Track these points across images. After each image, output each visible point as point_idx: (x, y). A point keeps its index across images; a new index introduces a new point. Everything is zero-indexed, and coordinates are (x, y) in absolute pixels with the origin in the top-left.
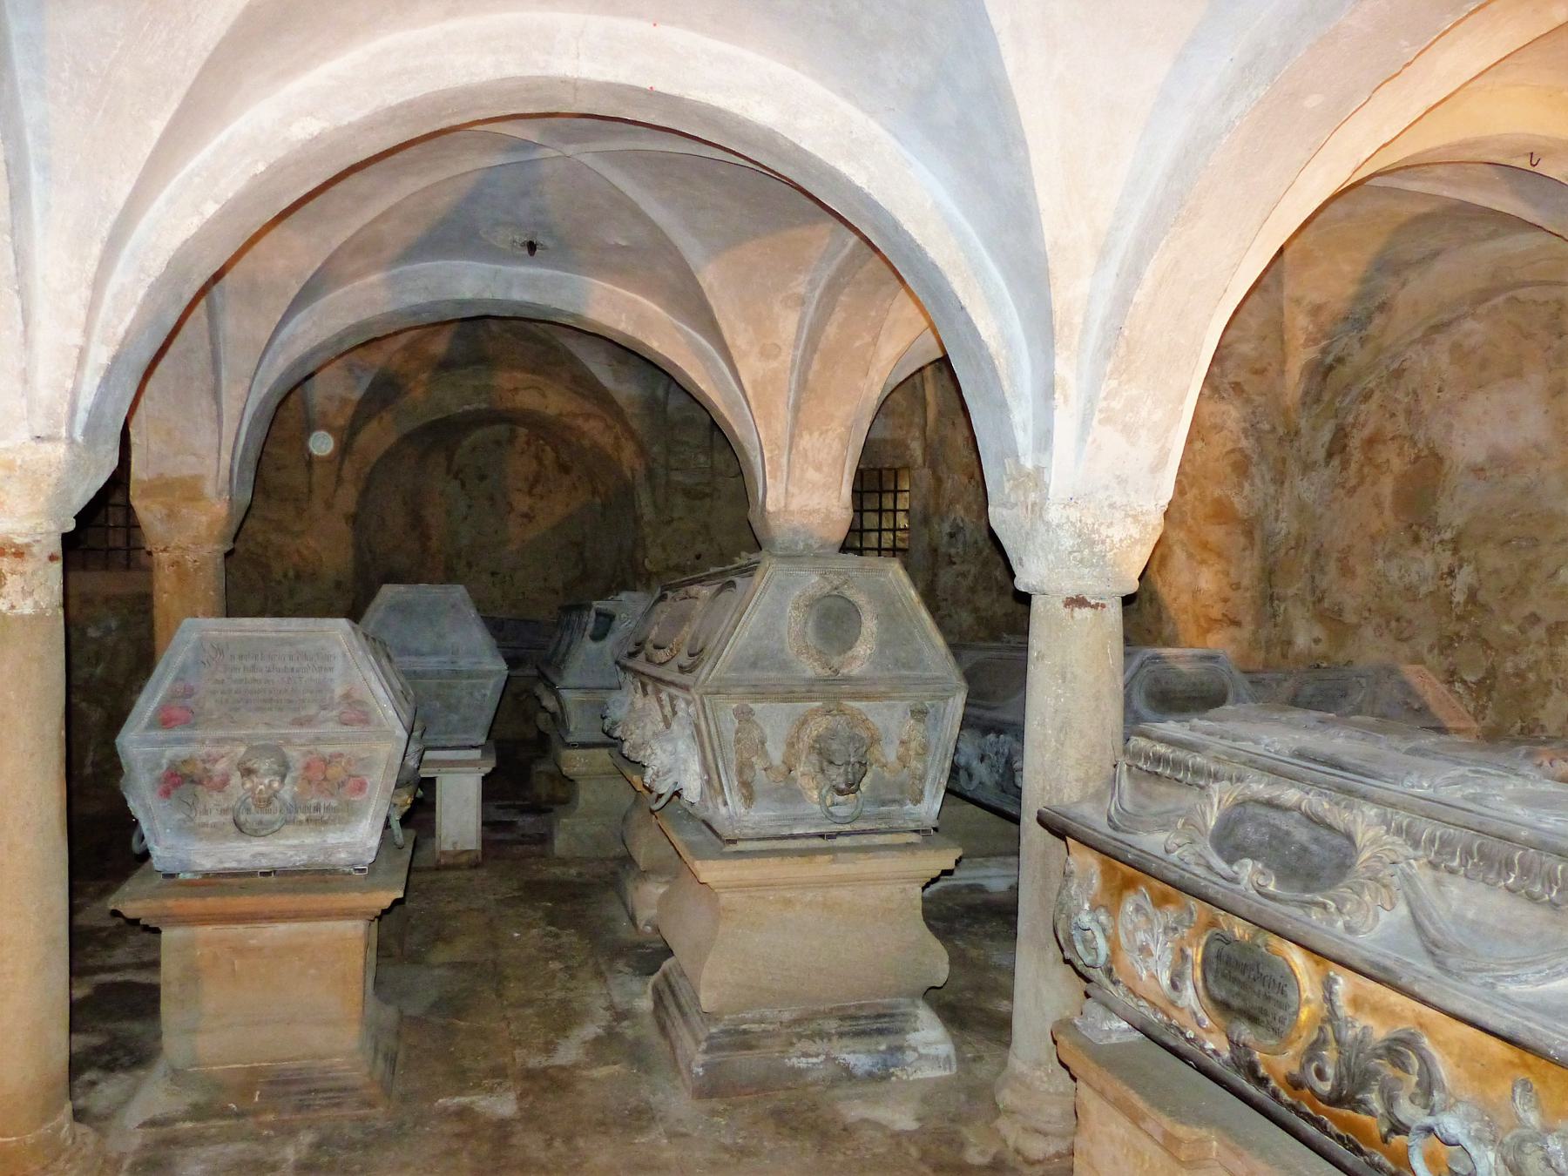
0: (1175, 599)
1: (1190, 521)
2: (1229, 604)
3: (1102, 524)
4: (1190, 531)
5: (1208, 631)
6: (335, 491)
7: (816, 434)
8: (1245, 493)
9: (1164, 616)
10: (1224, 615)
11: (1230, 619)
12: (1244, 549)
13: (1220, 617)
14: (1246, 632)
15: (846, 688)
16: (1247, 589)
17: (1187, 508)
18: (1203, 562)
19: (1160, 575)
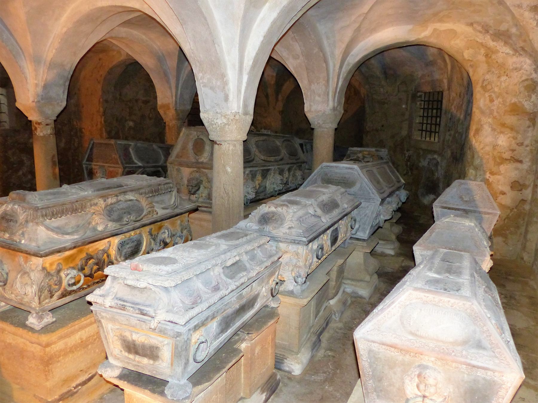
0: (482, 149)
1: (495, 114)
2: (516, 152)
3: (214, 119)
4: (495, 118)
5: (501, 163)
6: (276, 104)
7: (316, 84)
8: (532, 100)
9: (476, 157)
10: (511, 157)
11: (515, 159)
12: (529, 127)
13: (509, 158)
14: (525, 166)
15: (201, 165)
16: (527, 146)
17: (494, 108)
18: (502, 132)
19: (475, 138)
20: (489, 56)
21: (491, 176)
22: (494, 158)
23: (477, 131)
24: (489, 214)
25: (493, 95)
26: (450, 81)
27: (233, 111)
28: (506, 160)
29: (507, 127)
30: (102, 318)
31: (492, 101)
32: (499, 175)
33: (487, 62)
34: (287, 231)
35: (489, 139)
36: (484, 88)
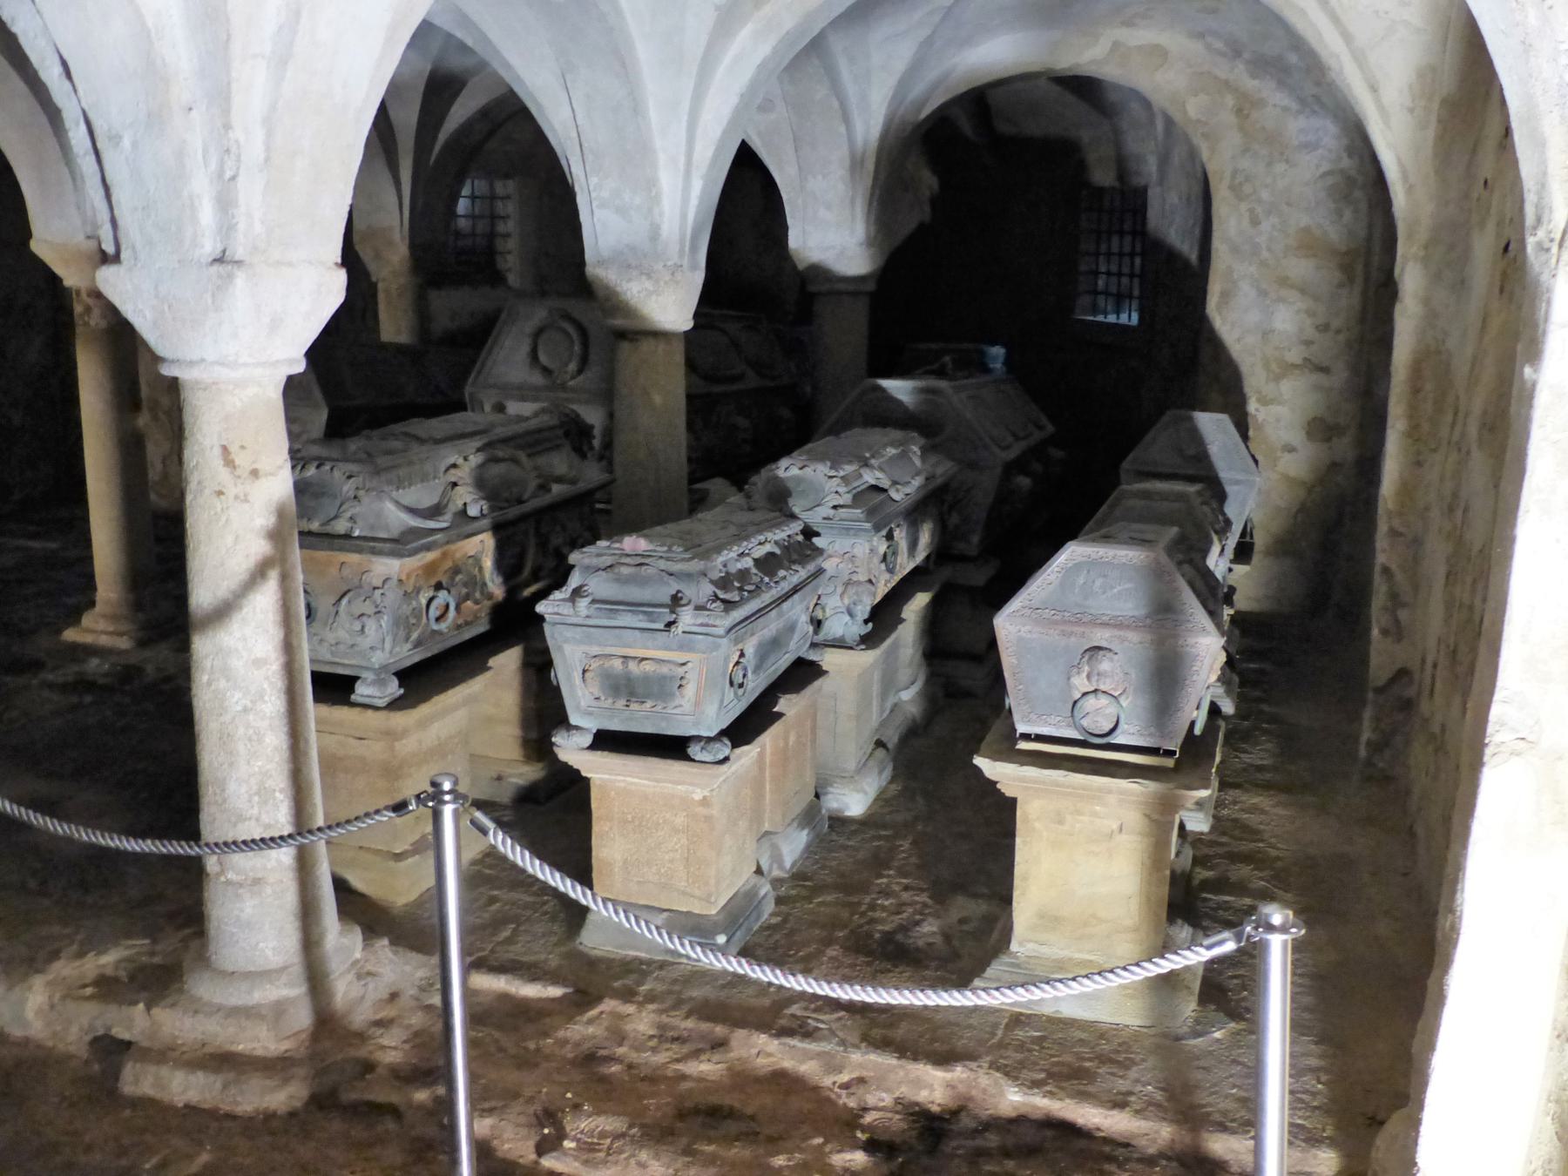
0: (1239, 340)
7: (820, 177)
16: (1338, 332)
17: (1262, 240)
18: (1281, 300)
19: (1220, 314)
20: (1245, 112)
21: (1262, 409)
22: (1266, 366)
23: (1226, 296)
24: (1237, 482)
25: (1259, 210)
26: (1164, 160)
27: (669, 263)
28: (1294, 366)
29: (1292, 287)
30: (567, 641)
31: (1255, 222)
32: (1280, 403)
33: (1241, 129)
34: (832, 512)
35: (1253, 317)
36: (1235, 189)
